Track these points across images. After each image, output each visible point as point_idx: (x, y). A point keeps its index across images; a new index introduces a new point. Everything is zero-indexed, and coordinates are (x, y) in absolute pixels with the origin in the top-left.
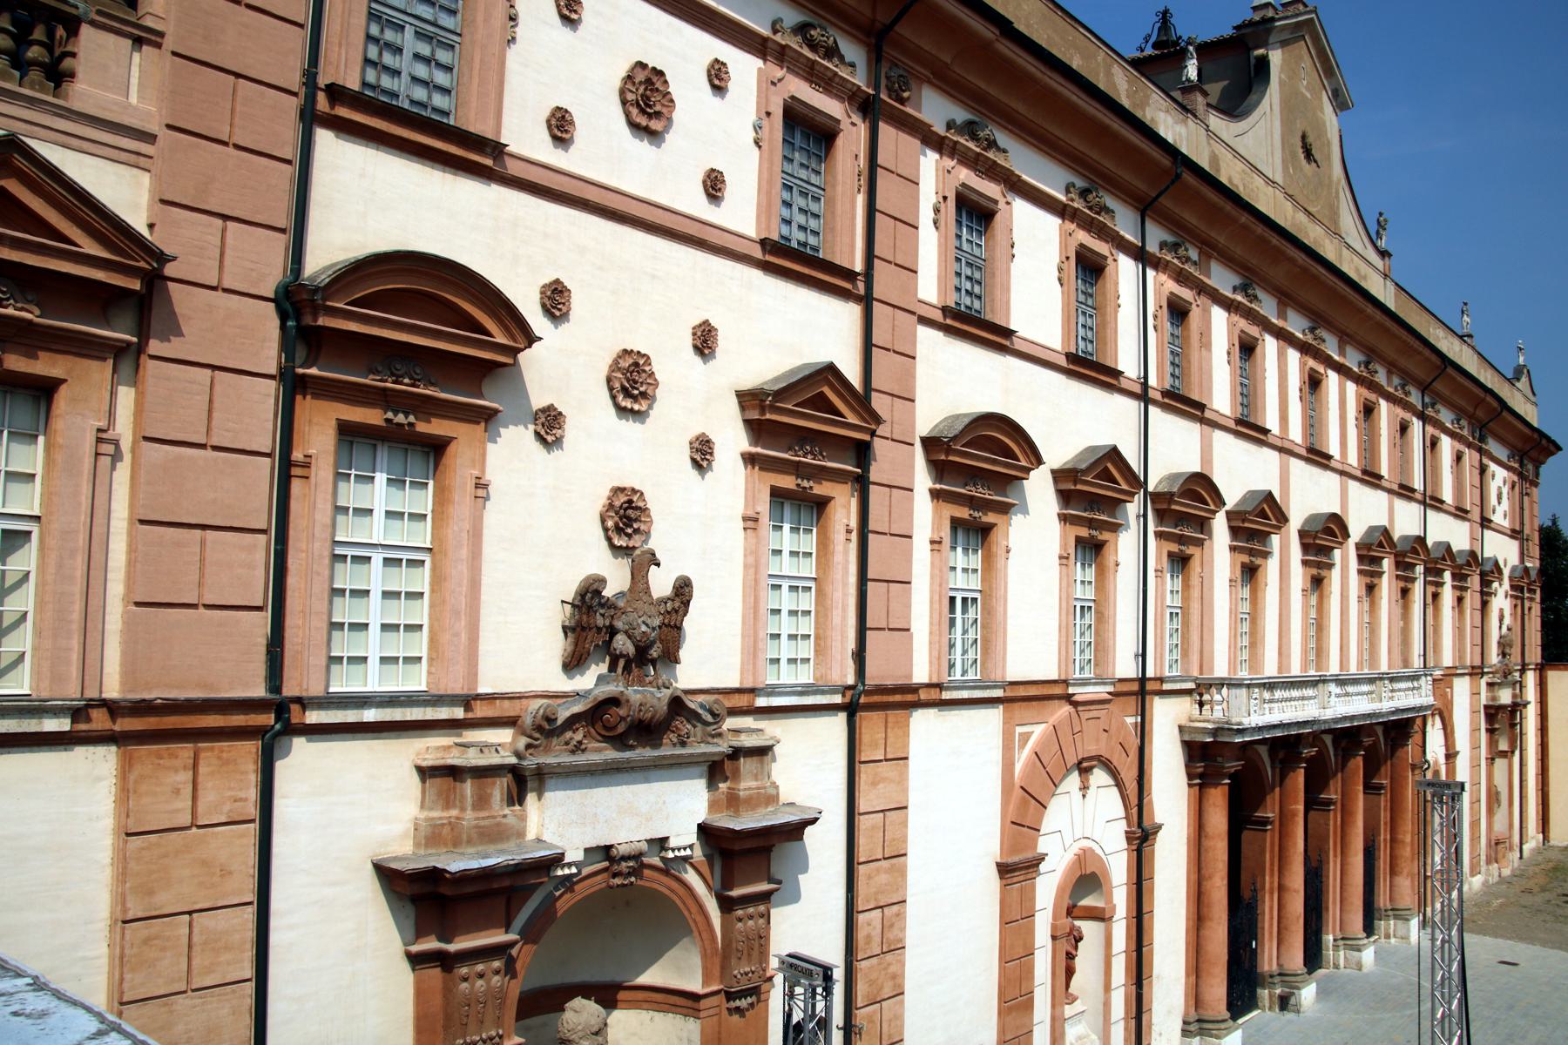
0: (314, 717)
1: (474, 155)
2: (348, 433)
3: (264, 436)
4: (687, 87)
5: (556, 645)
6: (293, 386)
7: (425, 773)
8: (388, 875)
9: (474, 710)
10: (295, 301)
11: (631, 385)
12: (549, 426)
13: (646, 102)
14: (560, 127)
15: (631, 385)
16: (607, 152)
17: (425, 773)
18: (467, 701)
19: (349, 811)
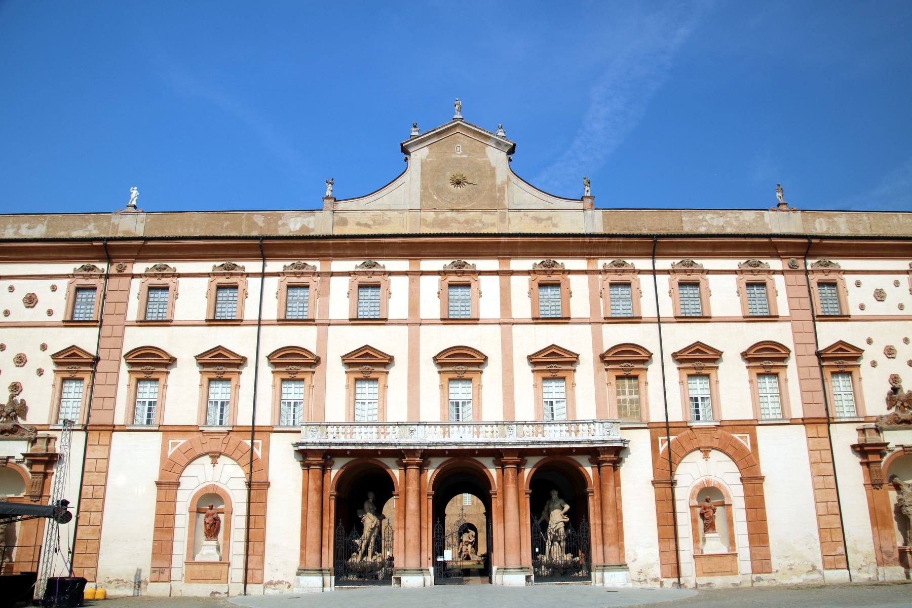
0: (835, 420)
1: (844, 317)
2: (833, 373)
3: (819, 376)
4: (889, 289)
5: (885, 406)
6: (821, 367)
7: (858, 430)
8: (853, 447)
9: (867, 419)
10: (818, 354)
11: (890, 352)
12: (874, 364)
13: (880, 295)
14: (862, 307)
15: (890, 352)
16: (874, 308)
17: (858, 430)
18: (866, 417)
19: (845, 437)
